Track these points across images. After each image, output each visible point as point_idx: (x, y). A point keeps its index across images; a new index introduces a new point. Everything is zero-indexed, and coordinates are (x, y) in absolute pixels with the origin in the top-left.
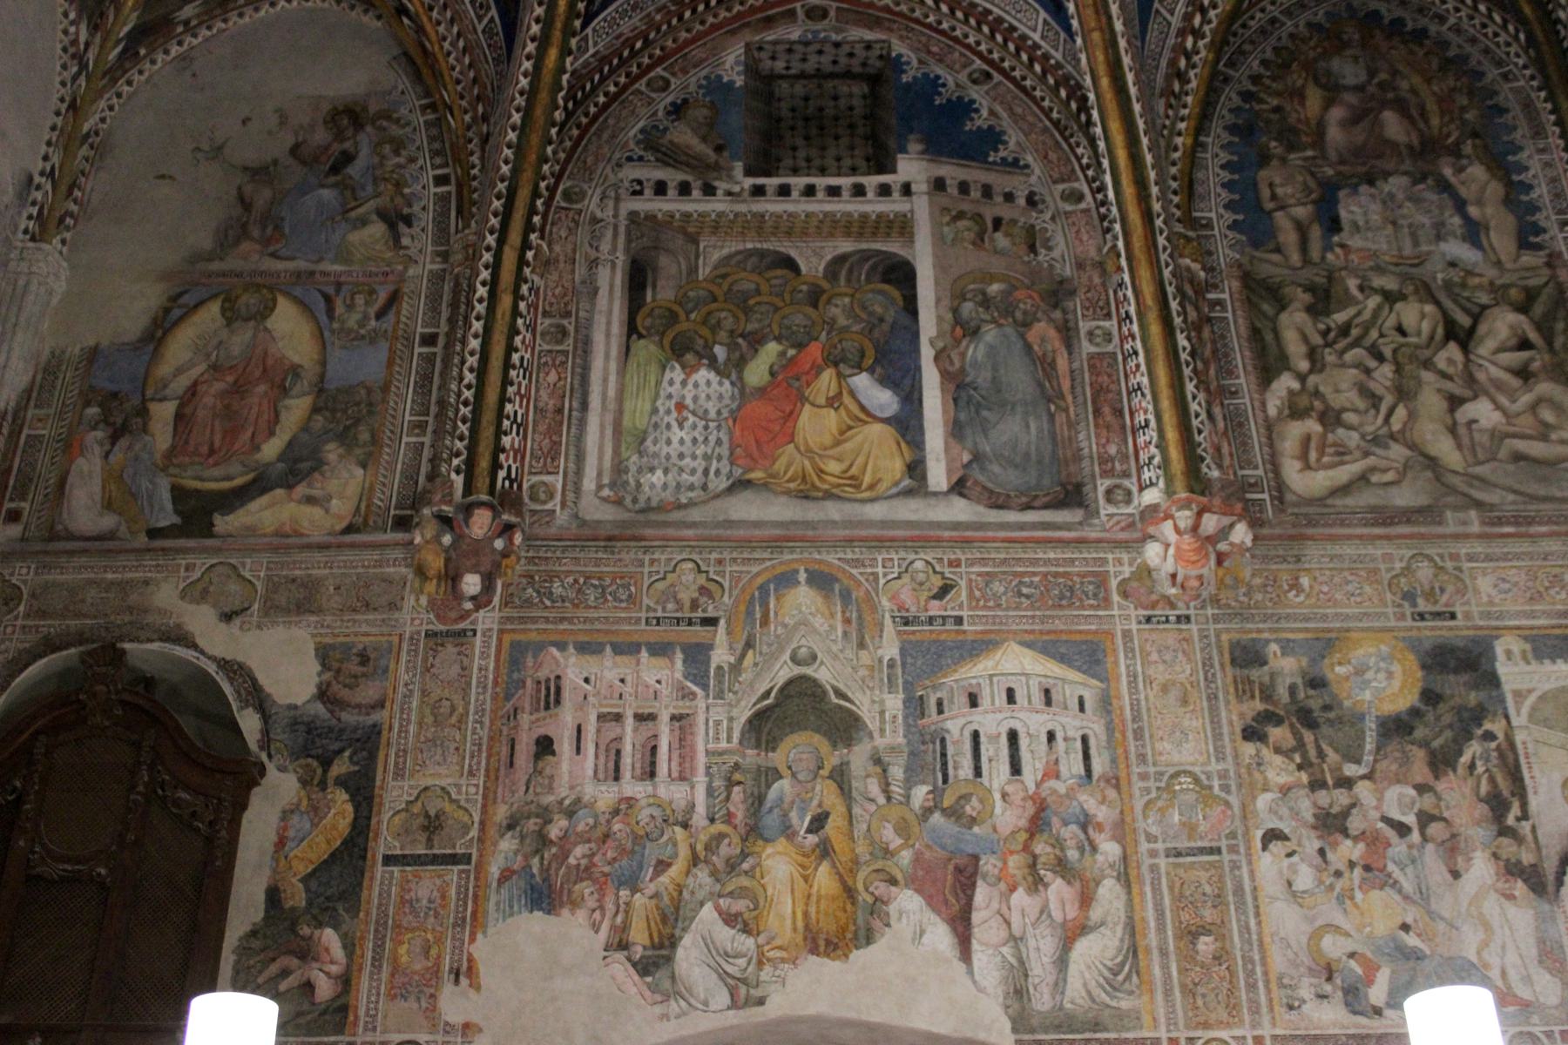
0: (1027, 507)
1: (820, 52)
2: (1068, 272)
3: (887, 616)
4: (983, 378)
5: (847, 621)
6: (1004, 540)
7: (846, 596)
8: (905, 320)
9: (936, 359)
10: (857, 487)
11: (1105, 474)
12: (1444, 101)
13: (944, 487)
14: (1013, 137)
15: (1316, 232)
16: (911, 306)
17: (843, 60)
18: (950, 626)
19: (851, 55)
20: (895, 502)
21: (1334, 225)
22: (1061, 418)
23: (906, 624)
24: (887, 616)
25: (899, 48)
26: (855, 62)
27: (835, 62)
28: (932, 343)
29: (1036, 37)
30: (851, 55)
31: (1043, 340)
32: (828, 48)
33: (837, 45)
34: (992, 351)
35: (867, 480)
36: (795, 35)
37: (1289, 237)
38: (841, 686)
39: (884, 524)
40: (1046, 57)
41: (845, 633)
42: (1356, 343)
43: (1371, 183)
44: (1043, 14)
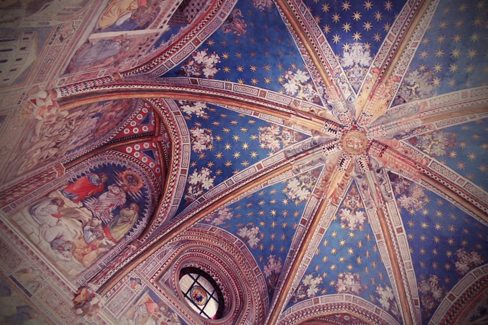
0: (72, 60)
1: (199, 4)
2: (120, 65)
3: (64, 22)
4: (110, 47)
5: (69, 10)
6: (67, 55)
7: (76, 10)
8: (136, 26)
9: (122, 35)
10: (104, 15)
11: (69, 79)
12: (103, 132)
13: (90, 38)
14: (153, 51)
15: (94, 114)
16: (139, 28)
17: (192, 7)
18: (50, 40)
19: (193, 11)
20: (94, 25)
21: (93, 117)
22: (88, 66)
23: (58, 28)
24: (64, 22)
25: (188, 25)
26: (190, 10)
27: (193, 5)
28: (126, 34)
29: (170, 59)
30: (193, 11)
31: (109, 60)
32: (198, 7)
33: (198, 10)
34: (115, 48)
35: (105, 17)
36: (207, 3)
37: (96, 109)
38: (49, 7)
39: (90, 21)
40: (165, 60)
41: (65, 9)
42: (66, 127)
43: (97, 122)
44: (175, 65)
